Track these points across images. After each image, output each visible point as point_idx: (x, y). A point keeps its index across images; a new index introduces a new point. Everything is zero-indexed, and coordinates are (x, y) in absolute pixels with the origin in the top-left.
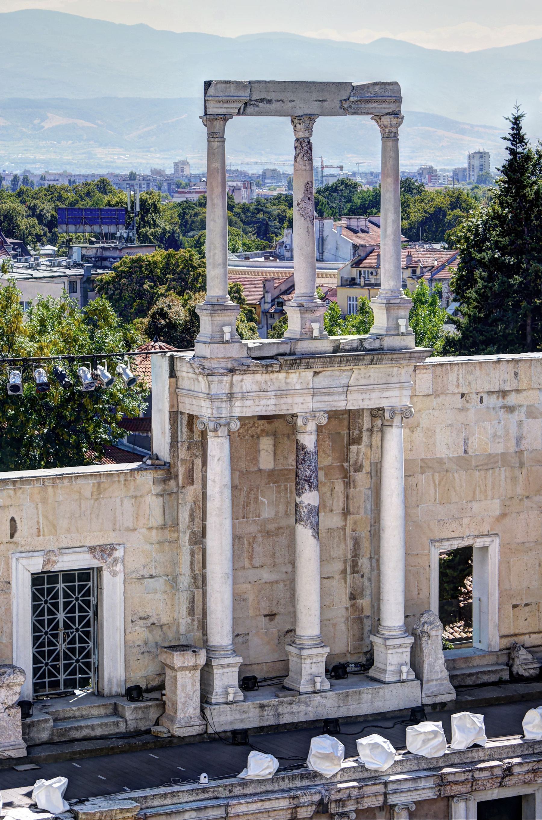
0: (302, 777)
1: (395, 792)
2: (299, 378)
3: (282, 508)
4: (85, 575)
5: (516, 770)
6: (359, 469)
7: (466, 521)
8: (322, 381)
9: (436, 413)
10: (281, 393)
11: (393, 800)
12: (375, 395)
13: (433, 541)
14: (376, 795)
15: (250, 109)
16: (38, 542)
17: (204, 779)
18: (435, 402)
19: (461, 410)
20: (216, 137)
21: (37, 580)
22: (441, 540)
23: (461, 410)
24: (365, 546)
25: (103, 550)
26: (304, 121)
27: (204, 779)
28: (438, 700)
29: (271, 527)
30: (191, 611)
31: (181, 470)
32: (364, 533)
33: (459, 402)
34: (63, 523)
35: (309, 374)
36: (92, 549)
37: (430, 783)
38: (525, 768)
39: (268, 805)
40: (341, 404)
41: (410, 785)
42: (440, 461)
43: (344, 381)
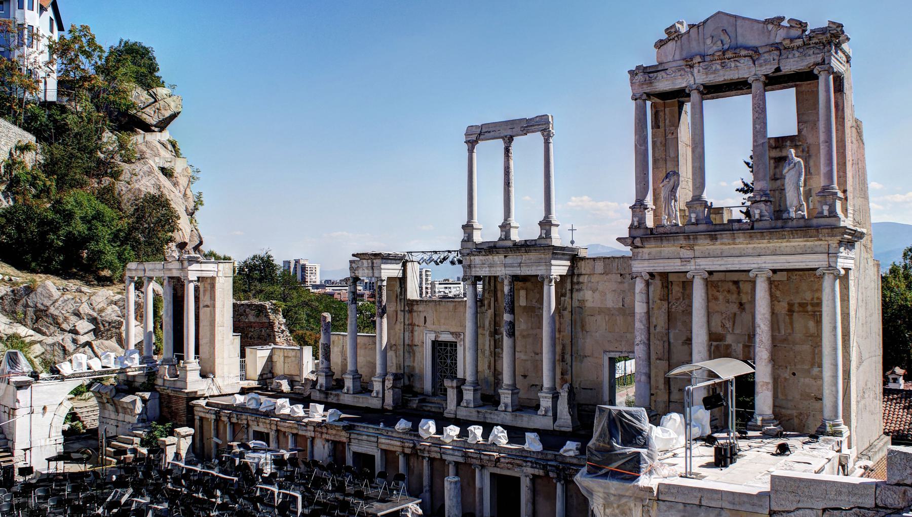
0: (415, 435)
1: (444, 453)
2: (498, 258)
3: (530, 324)
4: (454, 345)
5: (502, 460)
6: (565, 309)
7: (623, 343)
8: (509, 260)
9: (607, 284)
10: (491, 266)
11: (444, 457)
12: (533, 268)
13: (605, 352)
14: (436, 452)
15: (482, 137)
16: (433, 327)
17: (382, 425)
18: (605, 277)
19: (621, 283)
20: (471, 151)
21: (434, 343)
22: (609, 352)
23: (621, 283)
24: (568, 349)
25: (456, 334)
26: (509, 140)
27: (382, 425)
28: (563, 429)
29: (525, 333)
30: (489, 367)
31: (486, 302)
32: (568, 342)
33: (619, 278)
34: (442, 321)
35: (502, 257)
36: (452, 333)
37: (460, 454)
38: (507, 461)
39: (392, 442)
40: (517, 272)
41: (451, 452)
42: (609, 309)
43: (519, 261)
